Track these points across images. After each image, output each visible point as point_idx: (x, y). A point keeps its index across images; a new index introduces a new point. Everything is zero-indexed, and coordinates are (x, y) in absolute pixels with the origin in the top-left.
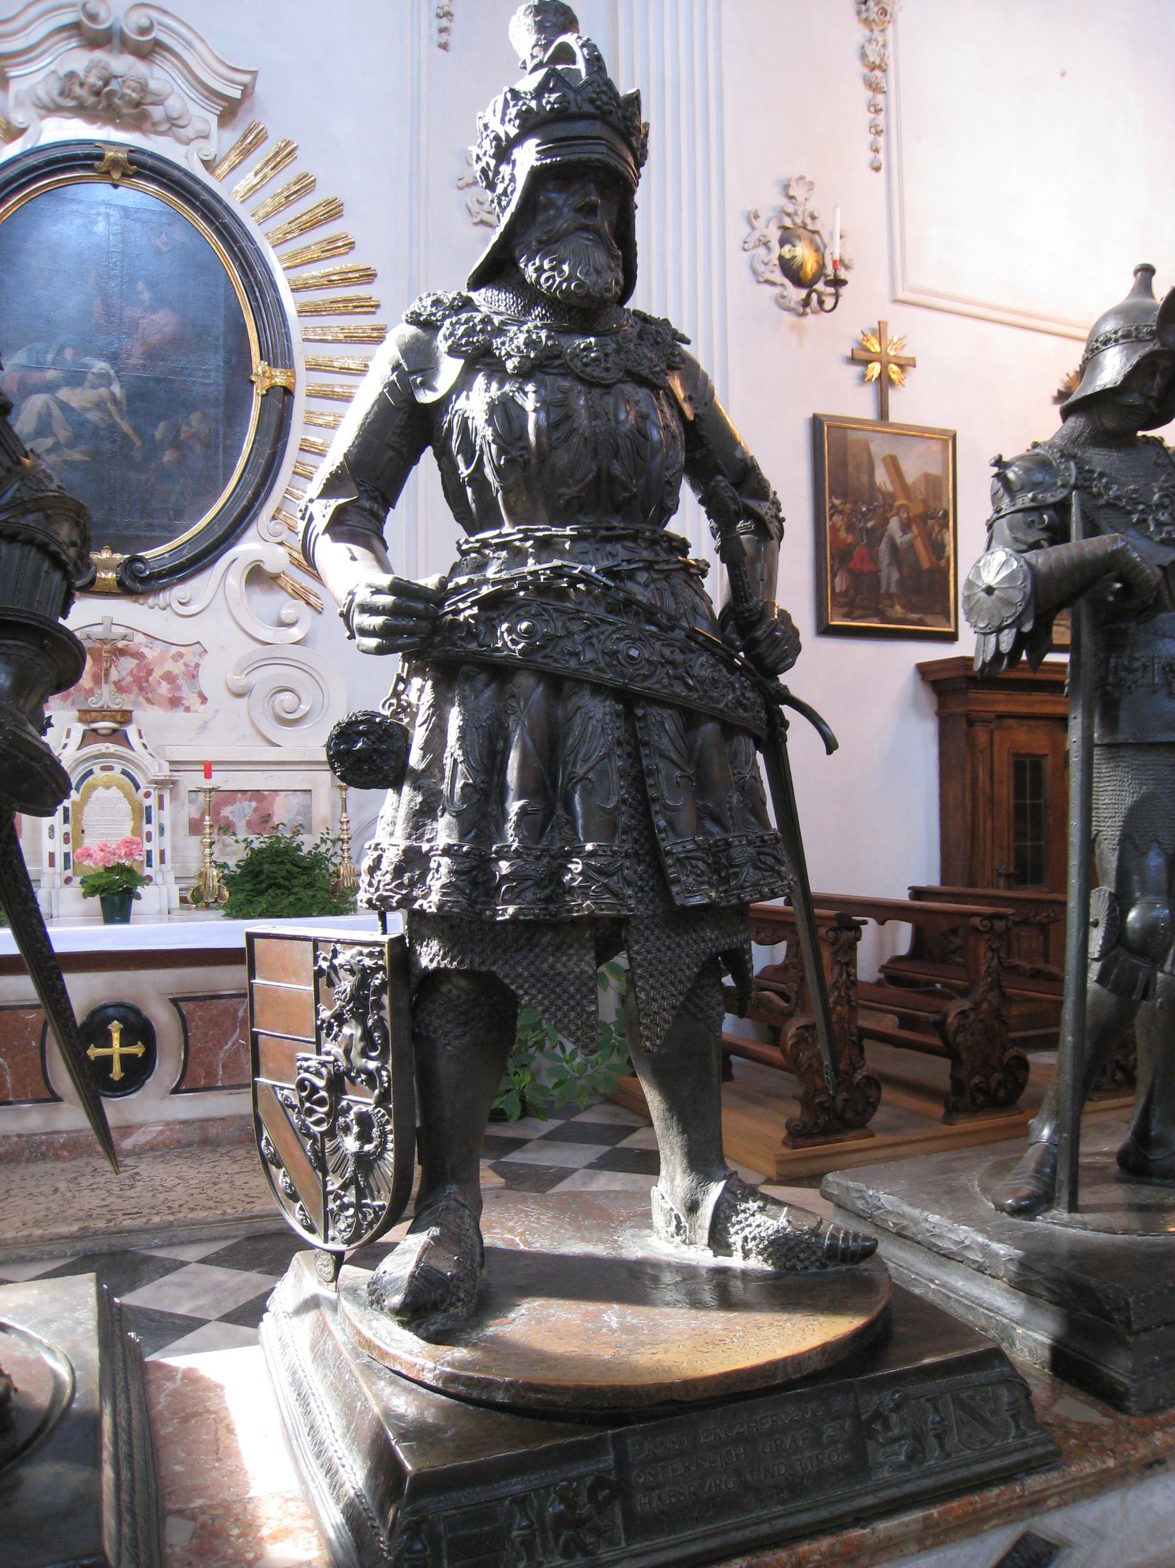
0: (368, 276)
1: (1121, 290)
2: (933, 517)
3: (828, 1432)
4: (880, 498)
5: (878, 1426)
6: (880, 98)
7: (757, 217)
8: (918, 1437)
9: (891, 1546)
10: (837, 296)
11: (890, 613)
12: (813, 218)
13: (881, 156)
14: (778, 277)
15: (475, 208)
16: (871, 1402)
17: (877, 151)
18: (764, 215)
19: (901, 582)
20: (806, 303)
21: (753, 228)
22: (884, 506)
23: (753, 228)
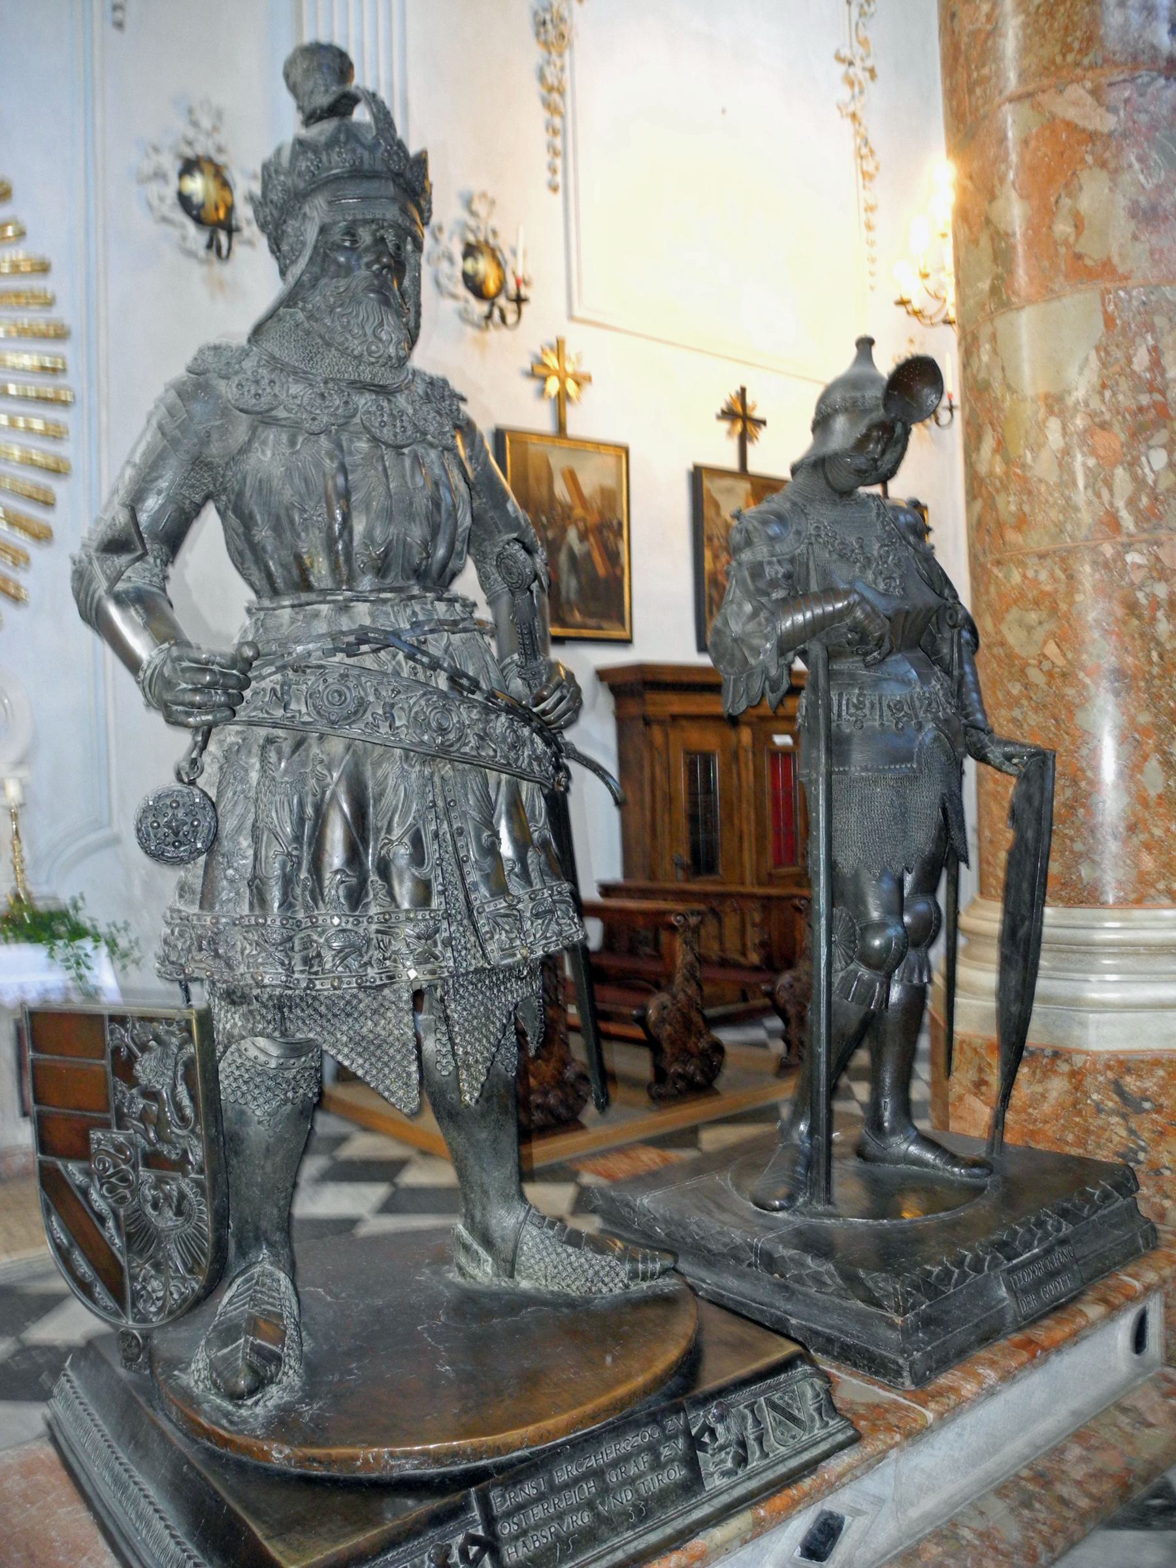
1: (842, 362)
2: (610, 527)
3: (665, 1452)
4: (559, 509)
5: (706, 1439)
6: (557, 121)
8: (743, 1444)
9: (724, 1549)
10: (519, 313)
11: (568, 619)
13: (559, 179)
14: (462, 290)
16: (698, 1419)
19: (581, 590)
20: (489, 317)
22: (565, 517)
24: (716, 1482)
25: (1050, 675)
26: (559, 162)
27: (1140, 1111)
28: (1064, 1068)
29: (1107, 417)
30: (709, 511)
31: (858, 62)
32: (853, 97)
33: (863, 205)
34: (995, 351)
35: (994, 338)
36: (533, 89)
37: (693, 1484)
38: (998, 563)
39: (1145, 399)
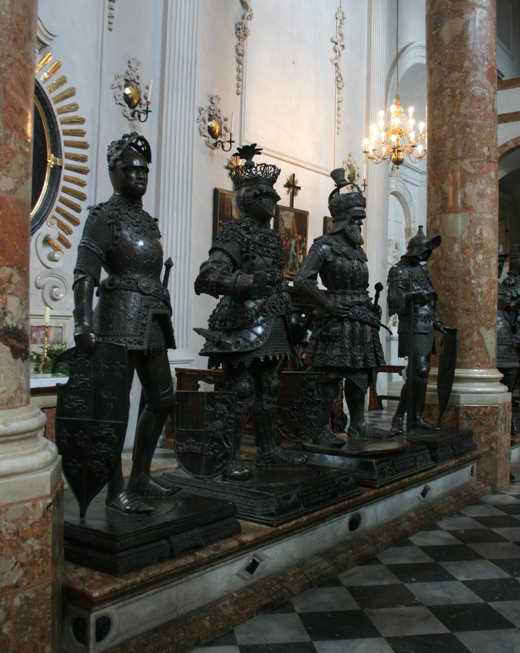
0: (81, 121)
7: (202, 110)
12: (219, 111)
13: (240, 89)
15: (117, 97)
17: (238, 87)
18: (205, 109)
20: (215, 145)
21: (200, 114)
23: (200, 114)
24: (418, 467)
25: (451, 309)
26: (240, 83)
27: (471, 419)
28: (453, 409)
29: (469, 245)
30: (281, 224)
31: (339, 43)
32: (336, 57)
33: (337, 100)
34: (441, 223)
35: (441, 219)
36: (234, 54)
37: (415, 466)
38: (438, 279)
39: (478, 242)
